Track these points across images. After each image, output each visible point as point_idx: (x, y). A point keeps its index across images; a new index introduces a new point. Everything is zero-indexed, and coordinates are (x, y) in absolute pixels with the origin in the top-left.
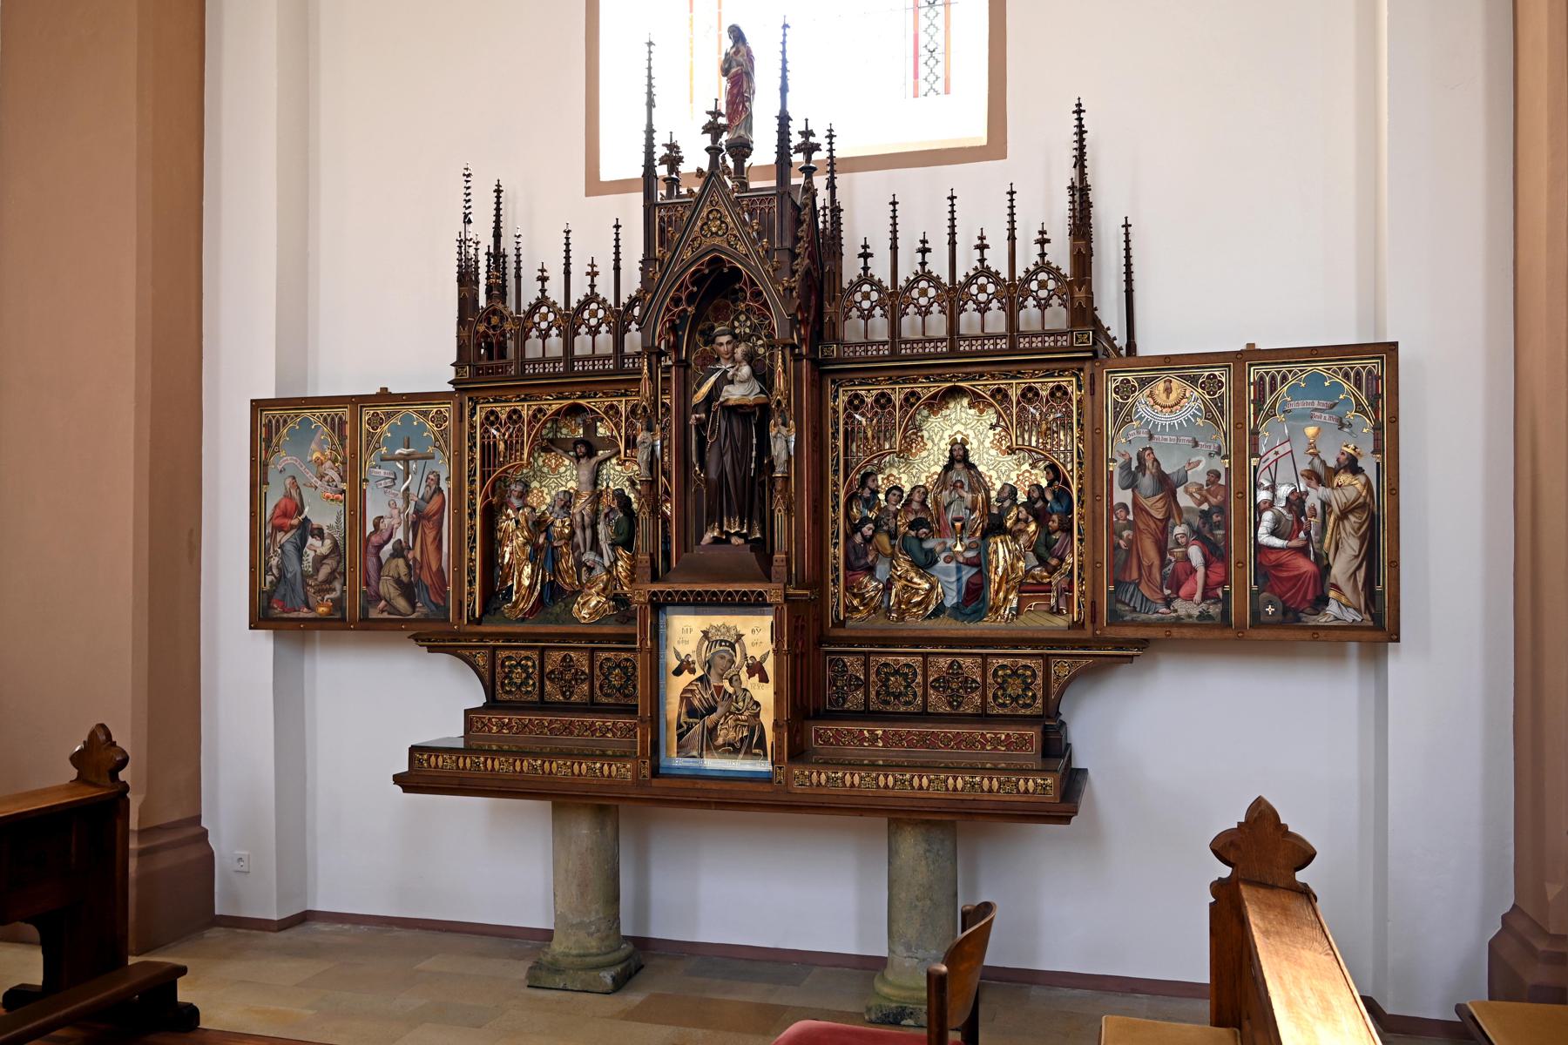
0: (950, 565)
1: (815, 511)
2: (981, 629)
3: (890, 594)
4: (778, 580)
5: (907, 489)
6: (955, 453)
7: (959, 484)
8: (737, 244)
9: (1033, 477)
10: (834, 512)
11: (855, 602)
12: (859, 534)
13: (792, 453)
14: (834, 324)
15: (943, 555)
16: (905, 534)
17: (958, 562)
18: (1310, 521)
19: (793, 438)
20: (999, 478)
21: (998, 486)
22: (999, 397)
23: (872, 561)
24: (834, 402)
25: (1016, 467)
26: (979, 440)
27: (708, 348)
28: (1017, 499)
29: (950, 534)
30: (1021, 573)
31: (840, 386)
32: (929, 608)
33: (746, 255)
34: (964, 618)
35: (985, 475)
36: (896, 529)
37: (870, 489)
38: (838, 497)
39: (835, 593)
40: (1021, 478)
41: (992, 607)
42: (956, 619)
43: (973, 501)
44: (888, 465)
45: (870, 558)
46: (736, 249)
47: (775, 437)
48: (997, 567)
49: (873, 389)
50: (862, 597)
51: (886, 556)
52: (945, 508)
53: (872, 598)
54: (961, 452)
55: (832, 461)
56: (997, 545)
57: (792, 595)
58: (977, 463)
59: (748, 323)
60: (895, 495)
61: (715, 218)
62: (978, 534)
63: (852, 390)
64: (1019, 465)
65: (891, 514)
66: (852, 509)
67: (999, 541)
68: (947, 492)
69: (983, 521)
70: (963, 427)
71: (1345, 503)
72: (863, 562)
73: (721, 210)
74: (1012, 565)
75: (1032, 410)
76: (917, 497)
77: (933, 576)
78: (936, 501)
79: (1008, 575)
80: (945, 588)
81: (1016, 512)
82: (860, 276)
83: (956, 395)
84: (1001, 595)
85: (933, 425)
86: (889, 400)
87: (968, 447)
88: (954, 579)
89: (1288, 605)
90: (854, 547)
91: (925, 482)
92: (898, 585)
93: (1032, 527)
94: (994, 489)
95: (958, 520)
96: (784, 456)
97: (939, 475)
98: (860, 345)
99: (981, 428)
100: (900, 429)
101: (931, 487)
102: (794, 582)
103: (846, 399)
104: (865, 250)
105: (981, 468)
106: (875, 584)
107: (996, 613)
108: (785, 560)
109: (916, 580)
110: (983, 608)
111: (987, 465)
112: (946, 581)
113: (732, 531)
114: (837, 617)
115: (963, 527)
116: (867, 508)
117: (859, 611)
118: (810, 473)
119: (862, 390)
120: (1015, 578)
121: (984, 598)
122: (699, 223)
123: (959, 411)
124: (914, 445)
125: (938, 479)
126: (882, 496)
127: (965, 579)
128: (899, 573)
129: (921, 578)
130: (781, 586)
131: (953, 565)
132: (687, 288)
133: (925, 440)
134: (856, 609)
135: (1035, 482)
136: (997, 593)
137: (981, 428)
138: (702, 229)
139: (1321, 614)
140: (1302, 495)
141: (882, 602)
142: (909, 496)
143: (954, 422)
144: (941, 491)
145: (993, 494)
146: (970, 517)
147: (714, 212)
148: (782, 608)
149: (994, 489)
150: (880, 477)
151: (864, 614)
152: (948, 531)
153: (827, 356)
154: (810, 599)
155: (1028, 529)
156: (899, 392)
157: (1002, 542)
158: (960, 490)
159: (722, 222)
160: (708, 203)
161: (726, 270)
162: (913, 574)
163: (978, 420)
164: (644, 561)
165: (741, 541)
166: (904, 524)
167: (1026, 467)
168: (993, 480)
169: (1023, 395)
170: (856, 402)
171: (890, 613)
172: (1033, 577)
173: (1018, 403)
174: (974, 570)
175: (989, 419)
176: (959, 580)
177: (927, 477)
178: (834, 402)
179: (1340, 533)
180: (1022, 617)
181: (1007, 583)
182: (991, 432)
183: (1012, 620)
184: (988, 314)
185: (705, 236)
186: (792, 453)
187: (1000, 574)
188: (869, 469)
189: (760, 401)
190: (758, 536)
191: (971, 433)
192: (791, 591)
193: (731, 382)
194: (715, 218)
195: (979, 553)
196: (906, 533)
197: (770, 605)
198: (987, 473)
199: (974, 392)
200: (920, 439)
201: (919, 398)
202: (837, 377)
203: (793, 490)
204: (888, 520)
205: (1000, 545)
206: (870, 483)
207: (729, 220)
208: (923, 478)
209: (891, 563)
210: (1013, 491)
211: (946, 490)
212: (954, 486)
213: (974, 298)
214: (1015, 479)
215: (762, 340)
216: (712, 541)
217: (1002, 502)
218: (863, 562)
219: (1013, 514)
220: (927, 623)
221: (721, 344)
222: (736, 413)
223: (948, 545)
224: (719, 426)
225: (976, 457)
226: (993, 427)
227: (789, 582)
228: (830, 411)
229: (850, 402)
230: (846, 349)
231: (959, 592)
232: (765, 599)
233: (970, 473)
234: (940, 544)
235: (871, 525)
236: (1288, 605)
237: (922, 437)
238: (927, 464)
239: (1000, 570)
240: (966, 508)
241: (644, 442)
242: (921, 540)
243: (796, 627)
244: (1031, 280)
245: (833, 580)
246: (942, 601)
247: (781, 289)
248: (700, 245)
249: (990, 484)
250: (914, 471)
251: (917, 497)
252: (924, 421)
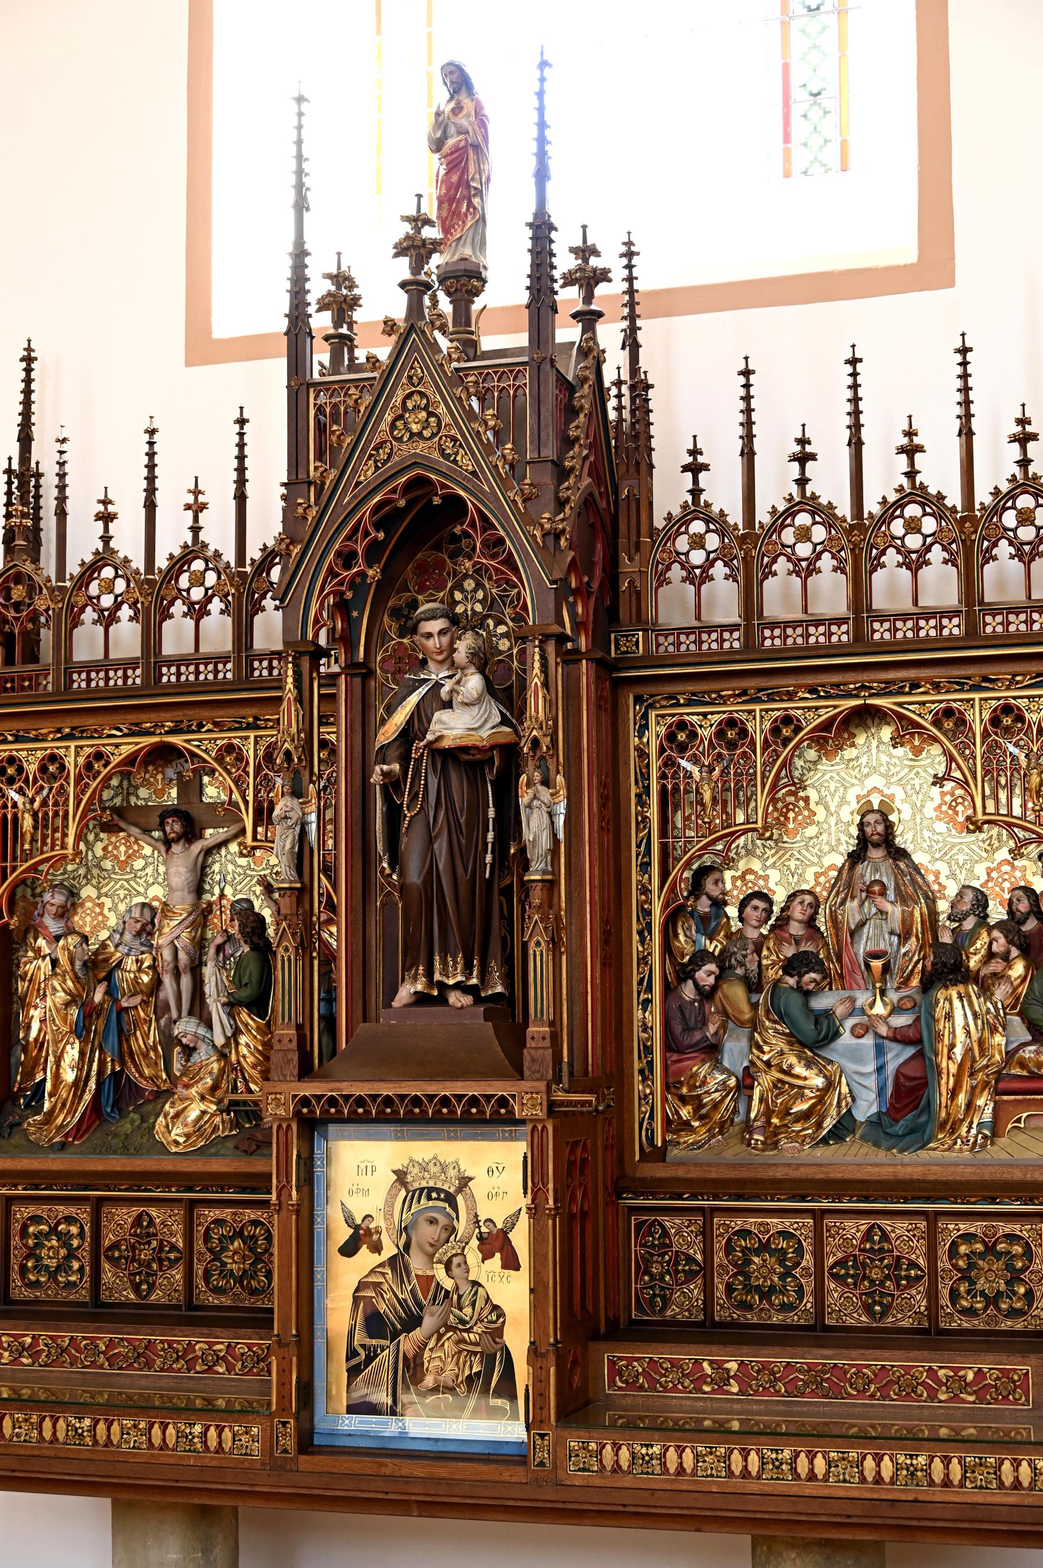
0: (863, 1041)
1: (606, 942)
2: (923, 1165)
3: (750, 1098)
4: (538, 1076)
5: (780, 897)
6: (869, 830)
7: (876, 888)
8: (457, 454)
9: (1018, 874)
10: (642, 942)
11: (685, 1112)
12: (690, 982)
13: (561, 836)
14: (638, 594)
15: (849, 1023)
16: (777, 983)
17: (877, 1035)
19: (561, 808)
20: (953, 875)
21: (952, 890)
22: (949, 724)
23: (716, 1033)
24: (640, 737)
25: (985, 855)
26: (913, 806)
27: (405, 641)
28: (987, 916)
29: (862, 982)
30: (998, 1057)
31: (652, 706)
32: (825, 1125)
33: (474, 473)
34: (892, 1141)
35: (927, 870)
36: (760, 973)
37: (710, 897)
38: (649, 913)
39: (646, 1096)
40: (994, 874)
41: (946, 1122)
42: (877, 1144)
43: (903, 921)
44: (743, 852)
45: (712, 1029)
46: (455, 461)
47: (529, 806)
48: (952, 1046)
49: (712, 713)
50: (697, 1103)
51: (741, 1024)
52: (852, 934)
53: (716, 1105)
54: (880, 828)
55: (638, 846)
56: (951, 1004)
57: (562, 1103)
58: (910, 848)
59: (480, 595)
60: (756, 908)
61: (417, 407)
62: (915, 982)
63: (673, 715)
64: (991, 850)
65: (751, 947)
66: (676, 935)
67: (955, 995)
68: (856, 903)
69: (924, 958)
70: (883, 781)
72: (697, 1036)
73: (428, 393)
74: (981, 1042)
75: (1011, 748)
76: (798, 912)
77: (831, 1062)
78: (834, 921)
79: (974, 1061)
80: (854, 1086)
81: (987, 940)
82: (685, 506)
83: (869, 722)
84: (962, 1099)
85: (827, 777)
86: (743, 732)
87: (893, 818)
88: (871, 1067)
90: (681, 1009)
91: (813, 883)
92: (765, 1081)
93: (1018, 969)
94: (944, 897)
95: (876, 955)
96: (545, 842)
97: (840, 871)
98: (688, 631)
99: (917, 782)
100: (763, 785)
101: (825, 894)
102: (565, 1079)
103: (663, 730)
104: (695, 459)
105: (917, 858)
106: (720, 1077)
107: (953, 1133)
108: (548, 1036)
109: (799, 1070)
110: (927, 1122)
111: (930, 850)
112: (856, 1073)
113: (451, 982)
114: (651, 1140)
115: (886, 969)
116: (704, 934)
117: (692, 1130)
118: (597, 872)
119: (693, 714)
120: (987, 1066)
121: (928, 1104)
122: (388, 417)
123: (874, 750)
124: (791, 815)
125: (837, 879)
126: (732, 911)
127: (891, 1068)
128: (765, 1058)
129: (808, 1066)
130: (542, 1086)
131: (868, 1041)
132: (367, 534)
133: (812, 806)
134: (686, 1125)
135: (1022, 884)
136: (954, 1094)
137: (917, 782)
138: (393, 426)
141: (735, 1111)
142: (783, 910)
143: (865, 771)
144: (843, 902)
145: (943, 906)
146: (898, 950)
147: (416, 397)
148: (544, 1127)
149: (944, 897)
150: (728, 875)
151: (702, 1135)
152: (859, 978)
153: (627, 652)
154: (596, 1110)
155: (1010, 973)
156: (762, 717)
157: (960, 998)
158: (879, 899)
159: (430, 414)
160: (404, 380)
161: (437, 501)
162: (793, 1059)
163: (912, 767)
164: (286, 1041)
165: (467, 1000)
166: (774, 964)
167: (1003, 854)
168: (942, 880)
169: (995, 721)
170: (682, 737)
171: (751, 1133)
172: (1022, 1065)
173: (985, 735)
174: (910, 1051)
175: (932, 764)
176: (880, 1069)
177: (817, 875)
178: (640, 737)
180: (1002, 1141)
181: (972, 1075)
182: (936, 790)
183: (983, 1146)
184: (924, 572)
185: (399, 440)
186: (561, 836)
187: (959, 1058)
188: (707, 860)
189: (502, 740)
190: (499, 989)
191: (898, 792)
192: (560, 1096)
193: (448, 705)
194: (417, 407)
195: (918, 1019)
196: (779, 980)
197: (522, 1122)
198: (930, 867)
199: (901, 717)
200: (802, 804)
201: (798, 729)
202: (645, 690)
203: (563, 905)
204: (745, 956)
205: (957, 1003)
206: (710, 887)
207: (442, 410)
208: (810, 875)
209: (751, 1038)
210: (981, 902)
211: (853, 898)
212: (869, 891)
213: (899, 542)
214: (984, 878)
215: (506, 624)
216: (413, 999)
217: (960, 920)
218: (697, 1036)
219: (981, 943)
220: (822, 1153)
221: (429, 635)
222: (457, 761)
223: (859, 1004)
224: (426, 785)
225: (909, 836)
226: (938, 781)
227: (557, 1079)
228: (633, 754)
229: (671, 737)
230: (661, 639)
231: (881, 1091)
232: (511, 1112)
233: (897, 866)
234: (843, 1001)
235: (712, 967)
237: (806, 800)
238: (815, 851)
239: (958, 1052)
240: (892, 933)
241: (286, 818)
242: (807, 994)
243: (571, 1164)
244: (1005, 509)
245: (641, 1072)
246: (849, 1110)
247: (538, 533)
248: (390, 455)
249: (936, 887)
250: (792, 864)
251: (798, 912)
252: (809, 770)
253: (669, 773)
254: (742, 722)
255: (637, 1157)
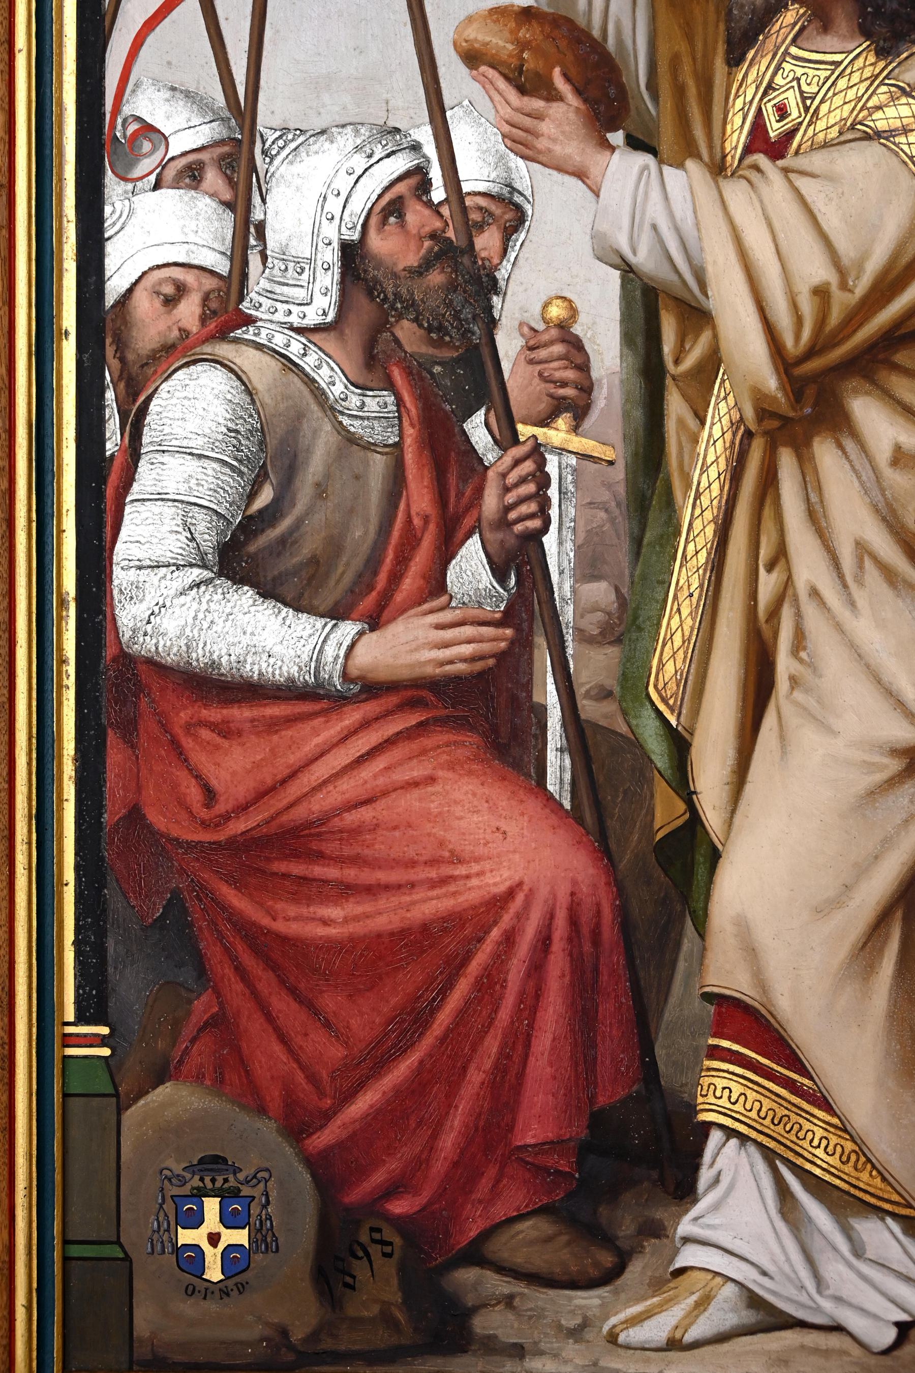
18: (537, 452)
71: (821, 293)
89: (355, 1195)
139: (635, 1270)
140: (471, 229)
179: (781, 555)
236: (355, 1195)
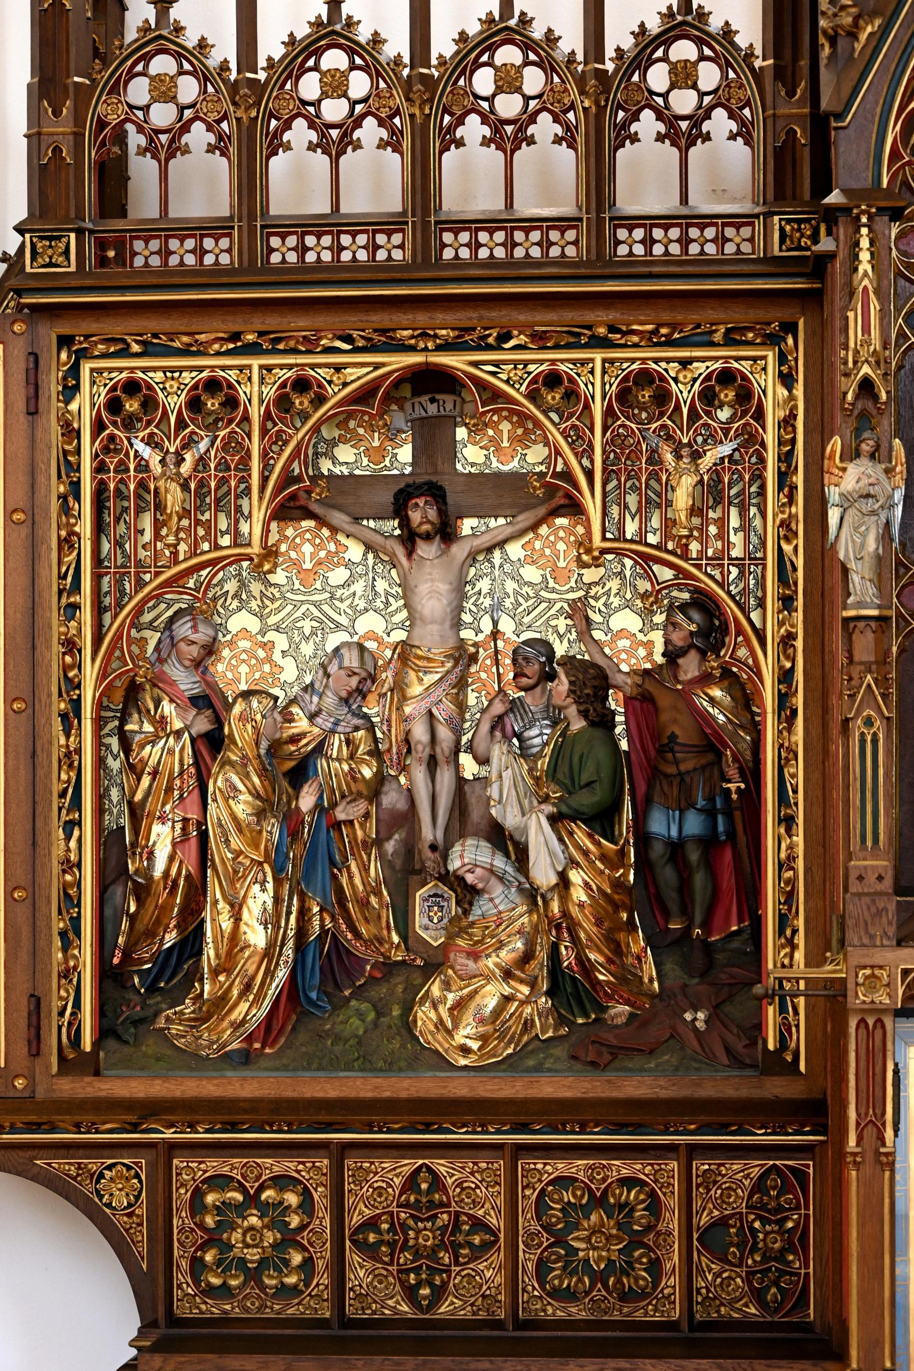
86: (232, 402)
114: (76, 1040)
201: (320, 400)
229: (114, 406)
253: (112, 462)
254: (230, 386)
255: (55, 1069)
